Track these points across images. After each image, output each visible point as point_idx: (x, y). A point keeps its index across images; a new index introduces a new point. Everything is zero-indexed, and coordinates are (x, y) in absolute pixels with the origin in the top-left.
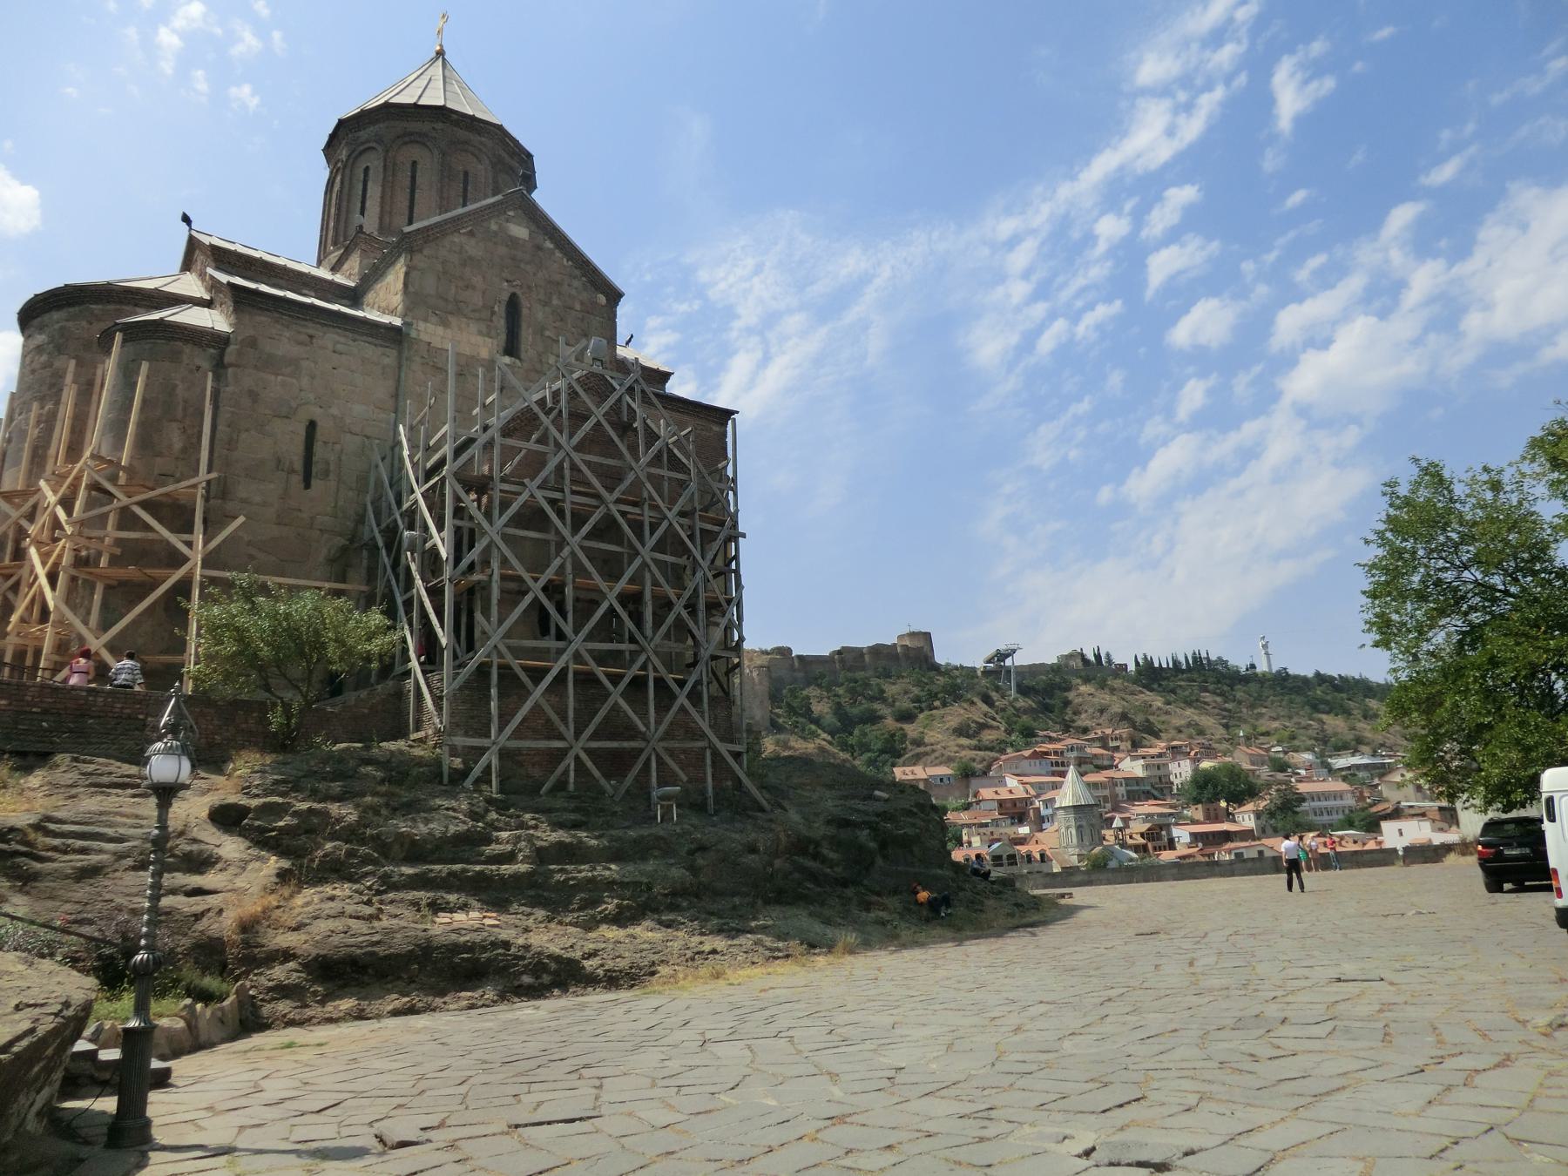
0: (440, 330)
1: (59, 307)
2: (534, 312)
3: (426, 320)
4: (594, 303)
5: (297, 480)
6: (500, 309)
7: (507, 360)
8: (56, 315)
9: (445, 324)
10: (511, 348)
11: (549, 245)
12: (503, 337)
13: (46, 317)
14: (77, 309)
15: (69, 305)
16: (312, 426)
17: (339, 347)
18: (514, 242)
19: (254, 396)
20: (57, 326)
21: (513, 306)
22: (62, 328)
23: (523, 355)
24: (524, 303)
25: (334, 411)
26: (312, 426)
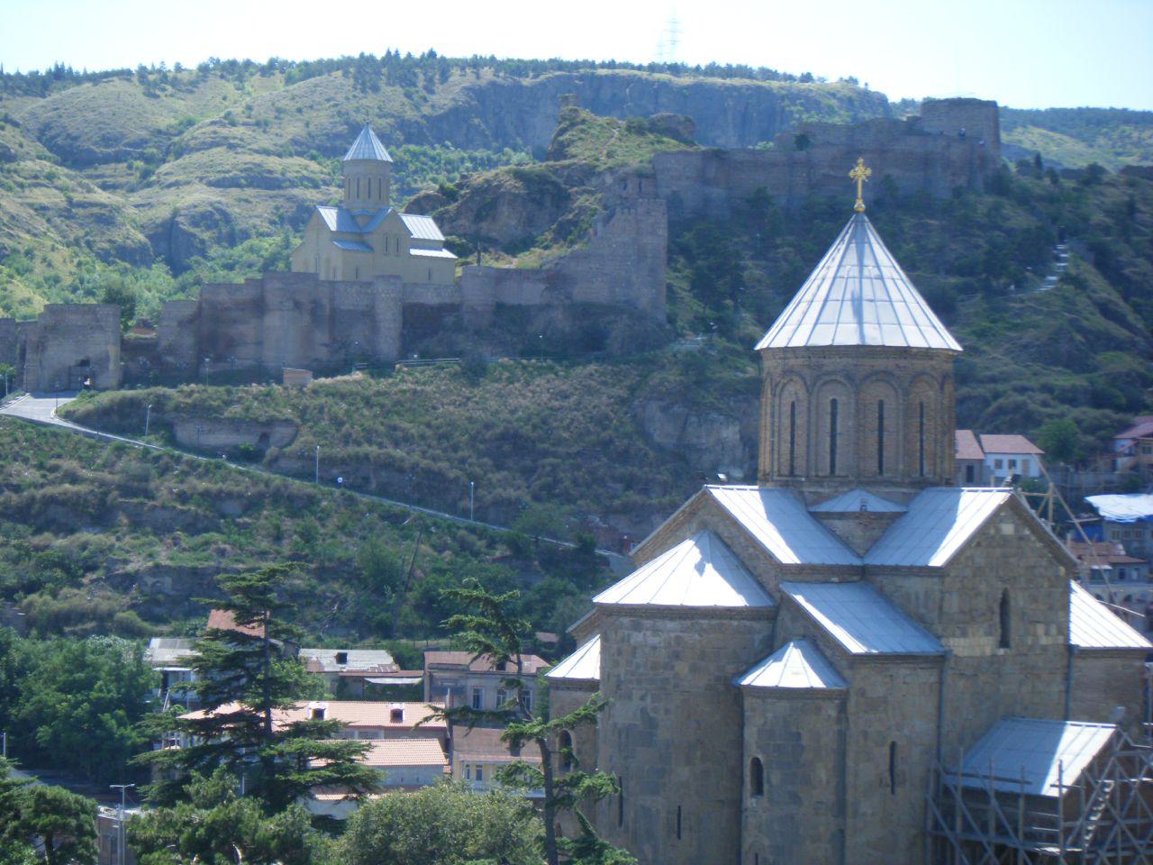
0: (962, 641)
1: (672, 619)
2: (1019, 601)
3: (954, 636)
4: (1057, 576)
5: (889, 789)
6: (997, 609)
7: (1001, 652)
8: (670, 625)
9: (964, 634)
10: (1004, 643)
11: (1027, 532)
12: (999, 631)
13: (660, 623)
14: (688, 622)
15: (680, 618)
16: (893, 746)
17: (908, 680)
18: (1005, 539)
19: (865, 735)
20: (673, 635)
21: (1004, 603)
22: (677, 638)
23: (1012, 644)
24: (1012, 595)
25: (906, 732)
26: (893, 746)
